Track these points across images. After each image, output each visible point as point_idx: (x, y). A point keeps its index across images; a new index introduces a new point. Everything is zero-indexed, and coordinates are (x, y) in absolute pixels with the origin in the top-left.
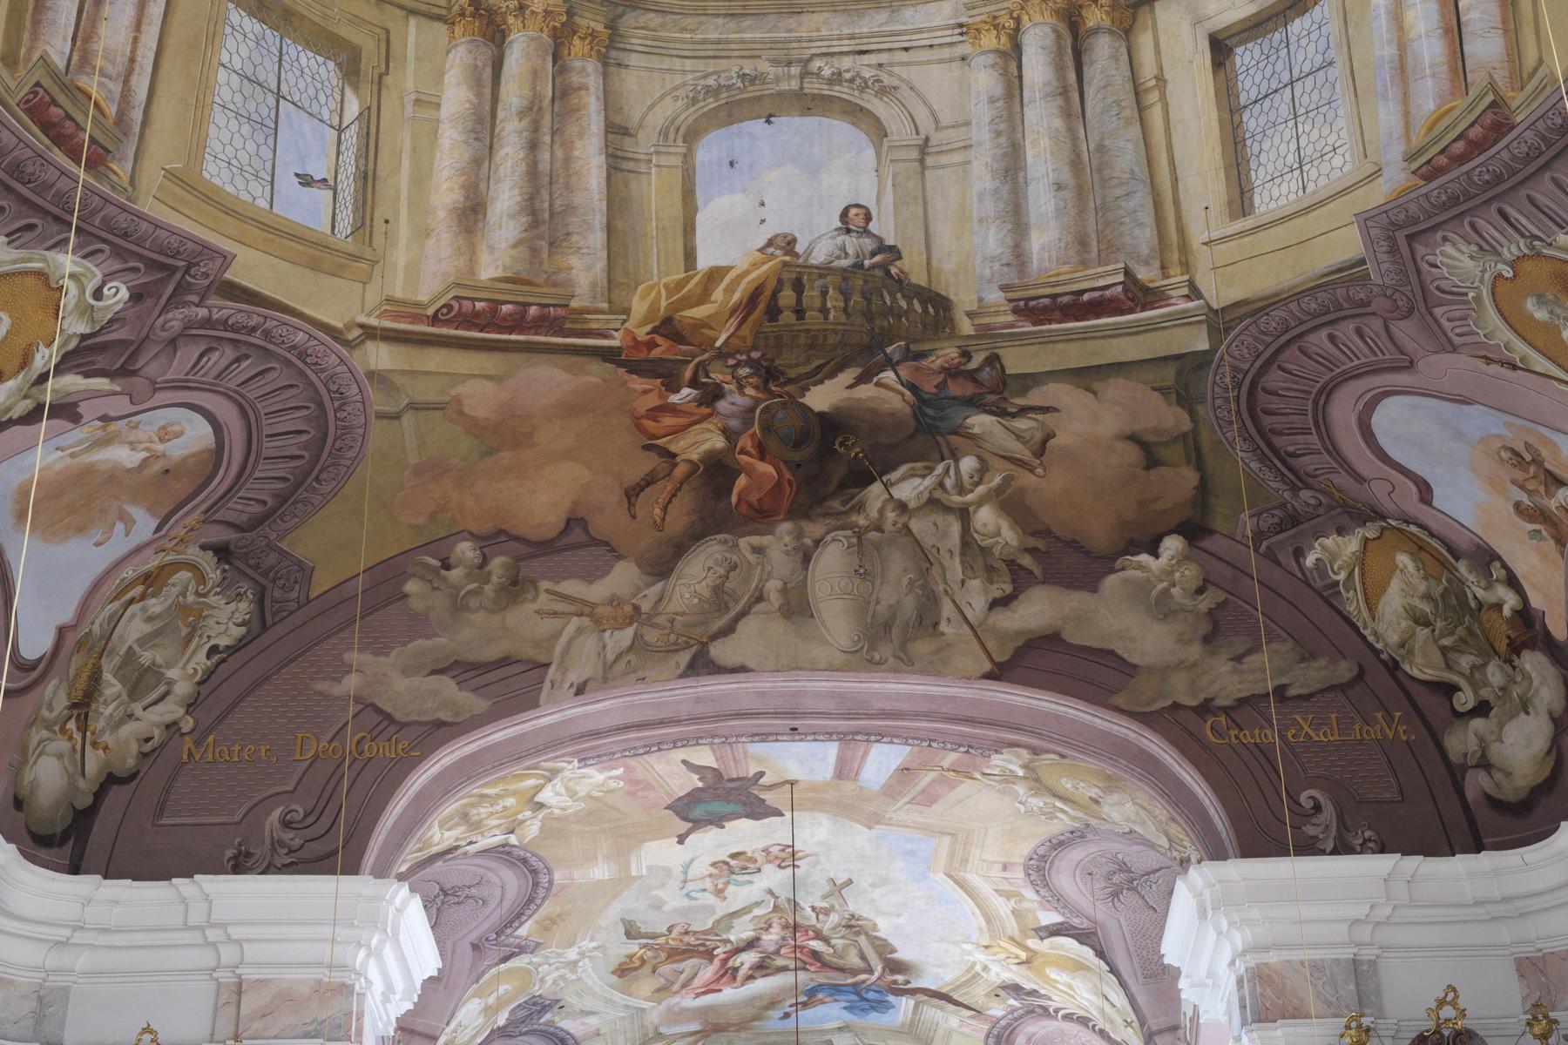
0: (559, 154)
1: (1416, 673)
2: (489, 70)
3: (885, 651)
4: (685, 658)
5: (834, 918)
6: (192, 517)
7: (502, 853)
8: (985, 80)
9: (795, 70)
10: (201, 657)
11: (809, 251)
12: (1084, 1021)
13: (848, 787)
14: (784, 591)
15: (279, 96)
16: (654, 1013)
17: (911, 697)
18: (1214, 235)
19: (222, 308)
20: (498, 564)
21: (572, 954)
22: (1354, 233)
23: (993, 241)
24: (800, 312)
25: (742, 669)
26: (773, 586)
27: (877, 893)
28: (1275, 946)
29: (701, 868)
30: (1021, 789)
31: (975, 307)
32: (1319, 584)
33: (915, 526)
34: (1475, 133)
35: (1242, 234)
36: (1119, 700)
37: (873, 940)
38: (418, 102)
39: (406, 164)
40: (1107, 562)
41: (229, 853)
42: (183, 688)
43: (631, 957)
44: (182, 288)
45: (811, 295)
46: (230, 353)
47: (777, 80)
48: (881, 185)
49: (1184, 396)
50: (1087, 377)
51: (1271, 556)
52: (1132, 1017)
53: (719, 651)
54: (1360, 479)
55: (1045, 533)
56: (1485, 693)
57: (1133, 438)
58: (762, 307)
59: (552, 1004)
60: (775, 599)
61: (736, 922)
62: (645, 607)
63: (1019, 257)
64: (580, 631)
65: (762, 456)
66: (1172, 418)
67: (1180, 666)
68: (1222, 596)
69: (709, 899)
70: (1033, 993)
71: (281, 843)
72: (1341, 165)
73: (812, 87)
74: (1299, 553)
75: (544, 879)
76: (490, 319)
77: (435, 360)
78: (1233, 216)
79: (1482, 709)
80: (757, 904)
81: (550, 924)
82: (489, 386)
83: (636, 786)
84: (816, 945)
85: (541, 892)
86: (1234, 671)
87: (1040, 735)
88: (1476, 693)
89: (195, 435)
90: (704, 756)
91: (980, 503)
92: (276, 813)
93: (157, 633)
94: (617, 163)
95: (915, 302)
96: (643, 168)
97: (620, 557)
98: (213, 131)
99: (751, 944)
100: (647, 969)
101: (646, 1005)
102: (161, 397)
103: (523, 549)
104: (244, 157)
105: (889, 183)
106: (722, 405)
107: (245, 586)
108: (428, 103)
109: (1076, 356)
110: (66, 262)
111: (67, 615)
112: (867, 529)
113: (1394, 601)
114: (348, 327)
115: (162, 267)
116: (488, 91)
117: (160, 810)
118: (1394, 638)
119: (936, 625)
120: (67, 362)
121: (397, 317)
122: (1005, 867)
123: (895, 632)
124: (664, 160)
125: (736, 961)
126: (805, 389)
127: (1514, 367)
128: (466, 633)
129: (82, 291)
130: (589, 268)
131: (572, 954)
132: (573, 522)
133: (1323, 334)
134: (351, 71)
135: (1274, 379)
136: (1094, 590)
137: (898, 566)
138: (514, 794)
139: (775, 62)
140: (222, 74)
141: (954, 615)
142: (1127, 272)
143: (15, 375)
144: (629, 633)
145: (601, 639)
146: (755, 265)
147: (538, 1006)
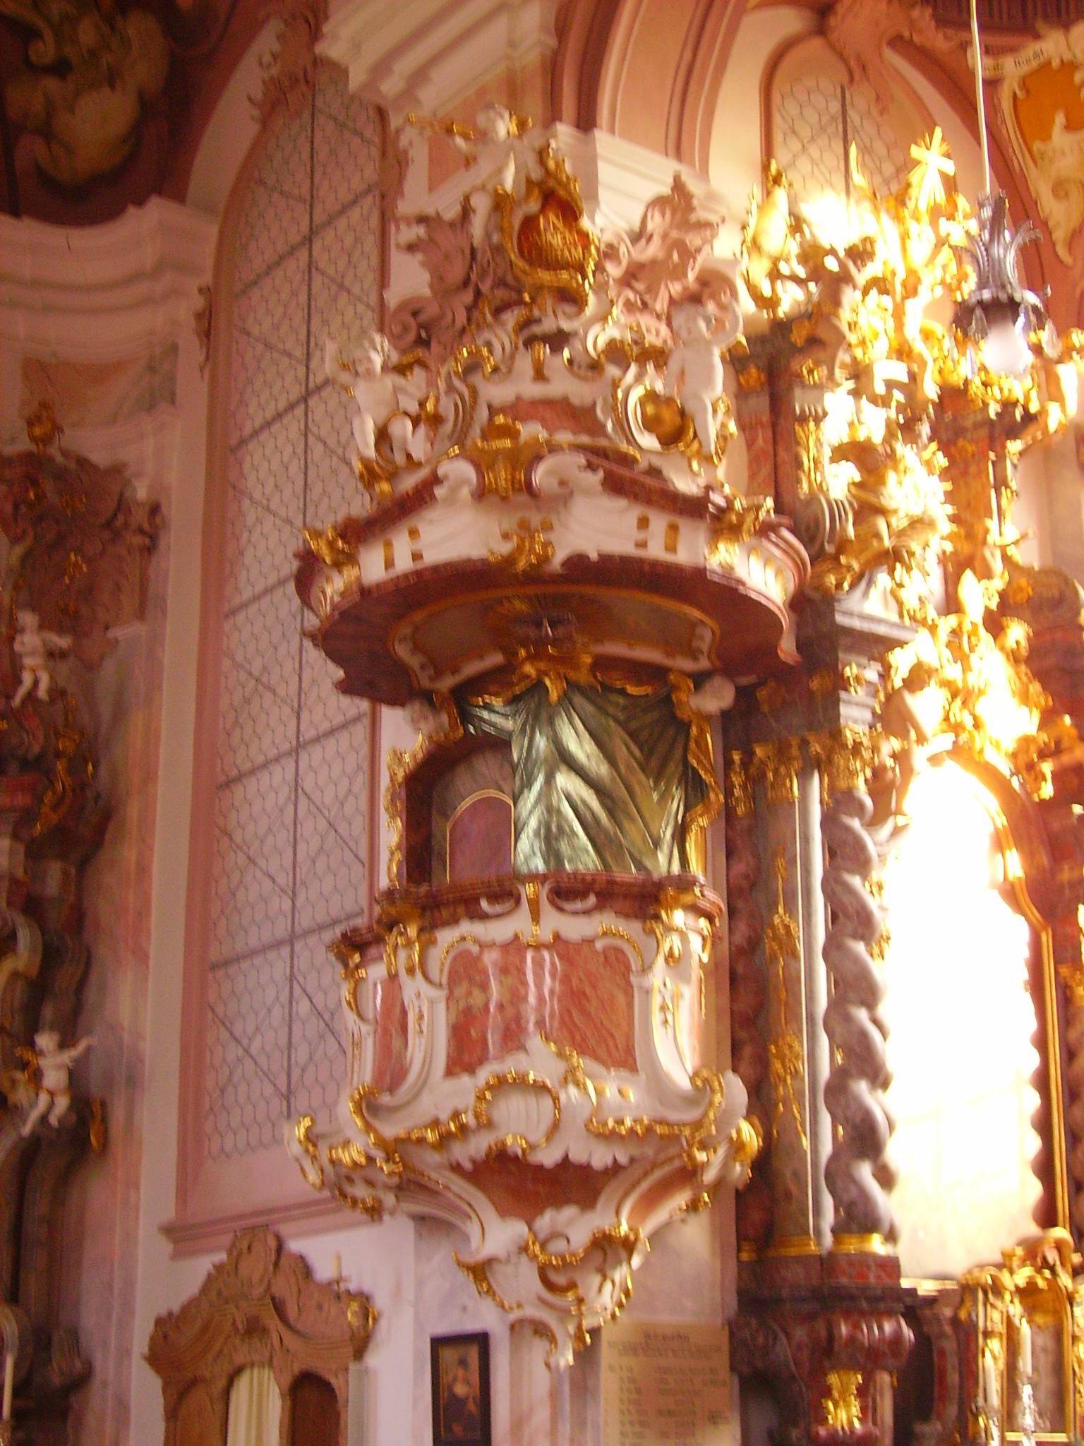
79: (61, 68)
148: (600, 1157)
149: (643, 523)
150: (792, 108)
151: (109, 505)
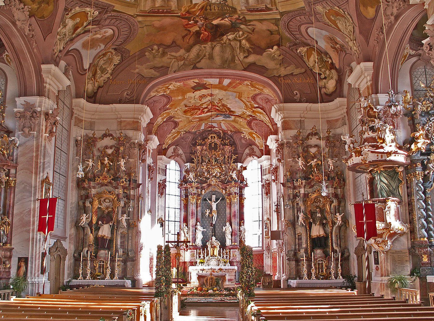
3: (226, 65)
4: (192, 66)
5: (220, 104)
7: (163, 95)
12: (262, 121)
13: (221, 85)
14: (209, 55)
19: (114, 14)
20: (161, 49)
21: (176, 110)
24: (211, 10)
26: (207, 54)
27: (227, 101)
31: (240, 10)
32: (300, 55)
33: (232, 43)
36: (265, 75)
37: (227, 108)
40: (264, 50)
42: (110, 71)
43: (186, 110)
44: (107, 11)
45: (212, 7)
46: (115, 20)
49: (277, 25)
50: (261, 21)
51: (292, 50)
53: (198, 65)
54: (306, 39)
55: (254, 45)
56: (326, 75)
57: (268, 30)
60: (207, 56)
64: (175, 61)
65: (205, 31)
67: (276, 69)
68: (283, 57)
69: (199, 101)
71: (127, 98)
74: (297, 50)
76: (158, 12)
77: (149, 19)
79: (325, 78)
80: (207, 102)
81: (172, 106)
82: (158, 22)
85: (170, 101)
86: (285, 70)
87: (252, 79)
88: (324, 75)
89: (110, 32)
90: (197, 81)
91: (243, 39)
97: (181, 48)
99: (206, 108)
101: (189, 117)
102: (104, 27)
103: (165, 47)
106: (198, 23)
107: (119, 54)
109: (258, 17)
110: (88, 9)
111: (91, 62)
112: (224, 44)
113: (312, 59)
114: (134, 15)
115: (103, 8)
117: (107, 93)
120: (89, 24)
123: (228, 62)
128: (156, 62)
129: (91, 13)
130: (174, 4)
131: (176, 110)
132: (174, 42)
133: (299, 17)
135: (291, 23)
136: (262, 55)
137: (228, 50)
138: (164, 87)
141: (238, 59)
143: (81, 27)
144: (183, 62)
145: (178, 63)
147: (171, 117)
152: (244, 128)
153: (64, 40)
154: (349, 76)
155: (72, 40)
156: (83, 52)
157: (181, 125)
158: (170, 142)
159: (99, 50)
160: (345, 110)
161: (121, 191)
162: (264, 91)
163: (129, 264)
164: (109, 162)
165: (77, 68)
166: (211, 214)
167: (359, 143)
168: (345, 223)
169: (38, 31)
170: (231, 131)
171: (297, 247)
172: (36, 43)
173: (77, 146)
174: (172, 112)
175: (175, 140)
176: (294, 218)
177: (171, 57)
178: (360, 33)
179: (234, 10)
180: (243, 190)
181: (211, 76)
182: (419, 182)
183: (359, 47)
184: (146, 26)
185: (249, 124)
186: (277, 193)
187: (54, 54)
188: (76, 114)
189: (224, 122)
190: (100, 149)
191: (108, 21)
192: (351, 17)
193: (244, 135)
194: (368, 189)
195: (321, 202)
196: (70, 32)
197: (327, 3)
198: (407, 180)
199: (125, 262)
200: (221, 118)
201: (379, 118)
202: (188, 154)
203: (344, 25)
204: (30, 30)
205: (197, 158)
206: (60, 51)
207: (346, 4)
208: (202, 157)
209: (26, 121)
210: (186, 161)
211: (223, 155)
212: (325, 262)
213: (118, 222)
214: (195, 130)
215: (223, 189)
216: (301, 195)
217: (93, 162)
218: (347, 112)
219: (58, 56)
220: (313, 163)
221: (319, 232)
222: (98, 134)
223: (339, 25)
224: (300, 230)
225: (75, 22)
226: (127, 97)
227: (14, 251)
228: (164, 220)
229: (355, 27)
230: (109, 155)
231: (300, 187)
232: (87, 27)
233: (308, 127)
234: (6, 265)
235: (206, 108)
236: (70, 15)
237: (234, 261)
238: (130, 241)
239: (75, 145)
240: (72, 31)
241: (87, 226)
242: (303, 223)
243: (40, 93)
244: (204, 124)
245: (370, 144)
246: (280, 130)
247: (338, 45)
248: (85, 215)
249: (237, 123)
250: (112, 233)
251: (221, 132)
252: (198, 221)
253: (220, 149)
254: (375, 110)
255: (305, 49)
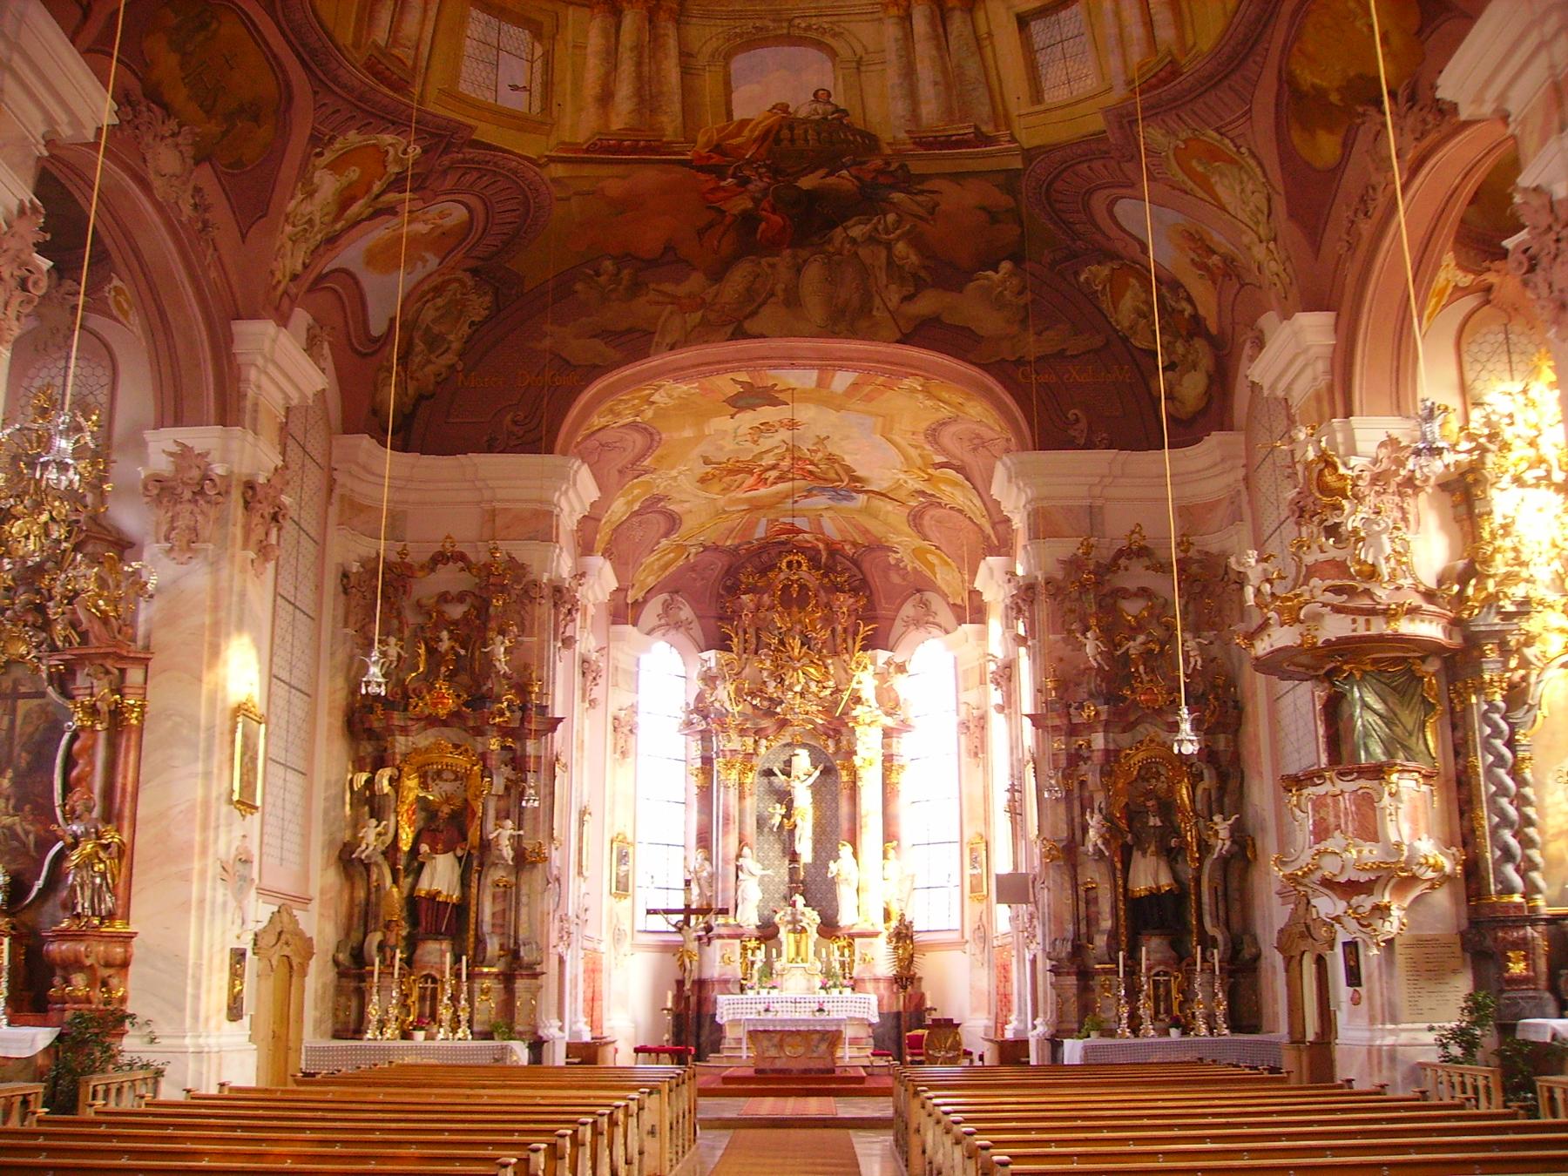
0: (654, 68)
1: (1138, 344)
2: (613, 30)
4: (730, 329)
5: (820, 455)
6: (458, 255)
7: (633, 426)
8: (892, 30)
9: (785, 24)
10: (466, 327)
11: (796, 112)
12: (960, 511)
13: (824, 392)
14: (785, 290)
15: (499, 49)
16: (722, 500)
17: (857, 351)
18: (1022, 112)
19: (471, 153)
20: (625, 273)
21: (674, 473)
22: (1100, 117)
23: (900, 107)
24: (792, 140)
25: (763, 336)
26: (780, 287)
27: (843, 443)
28: (1046, 498)
29: (744, 429)
30: (920, 396)
33: (862, 252)
34: (1162, 74)
35: (1038, 113)
38: (575, 47)
39: (569, 76)
40: (969, 275)
41: (485, 438)
42: (456, 345)
45: (799, 132)
46: (475, 175)
47: (775, 29)
48: (836, 78)
50: (956, 177)
52: (985, 513)
54: (1109, 238)
56: (1175, 358)
57: (983, 209)
58: (770, 139)
59: (666, 498)
60: (780, 293)
61: (765, 456)
62: (708, 299)
63: (915, 115)
64: (671, 313)
65: (774, 212)
66: (1005, 200)
69: (749, 445)
70: (933, 495)
72: (1090, 83)
73: (797, 32)
74: (1076, 274)
75: (657, 438)
76: (618, 149)
77: (587, 170)
78: (1033, 104)
83: (705, 391)
84: (810, 467)
85: (655, 444)
89: (458, 214)
90: (743, 377)
91: (898, 240)
92: (509, 417)
93: (442, 316)
94: (686, 71)
95: (858, 137)
96: (701, 72)
97: (694, 269)
98: (464, 69)
99: (774, 467)
100: (716, 480)
104: (480, 79)
105: (840, 80)
106: (751, 187)
108: (580, 47)
109: (948, 167)
110: (388, 138)
113: (1128, 303)
116: (613, 40)
118: (1126, 324)
119: (871, 311)
121: (566, 151)
122: (913, 434)
124: (713, 68)
125: (767, 475)
126: (797, 179)
127: (1186, 193)
132: (669, 248)
133: (1085, 165)
134: (537, 35)
139: (774, 21)
140: (468, 41)
142: (976, 127)
144: (700, 313)
146: (766, 118)
147: (658, 499)
148: (1363, 877)
149: (1354, 621)
150: (1475, 348)
151: (1222, 572)
152: (898, 533)
153: (307, 240)
154: (1252, 359)
155: (331, 241)
156: (370, 281)
157: (689, 523)
158: (651, 581)
159: (419, 273)
160: (1241, 473)
161: (494, 744)
162: (967, 409)
163: (520, 984)
164: (453, 648)
165: (348, 333)
166: (789, 819)
167: (1289, 582)
168: (1243, 848)
169: (221, 213)
170: (854, 544)
171: (1083, 929)
172: (216, 250)
173: (345, 591)
174: (660, 482)
175: (667, 573)
176: (1073, 830)
177: (661, 299)
178: (1292, 215)
179: (870, 142)
180: (895, 740)
181: (792, 361)
182: (1493, 707)
183: (1287, 264)
184: (575, 194)
185: (916, 519)
186: (1012, 749)
187: (275, 288)
188: (343, 486)
189: (830, 513)
190: (424, 601)
191: (449, 182)
192: (1261, 165)
193: (898, 556)
194: (1321, 731)
195: (1163, 778)
196: (327, 214)
197: (1180, 118)
198: (1451, 701)
199: (508, 979)
200: (821, 501)
201: (1355, 496)
202: (713, 621)
203: (1238, 189)
204: (195, 206)
205: (741, 633)
206: (295, 277)
207: (1241, 121)
208: (758, 629)
209: (179, 507)
210: (702, 644)
211: (828, 621)
212: (1176, 978)
213: (486, 846)
214: (737, 542)
215: (829, 737)
216: (1096, 753)
217: (402, 647)
218: (1246, 479)
219: (285, 293)
220: (1134, 646)
221: (1156, 879)
222: (419, 554)
223: (1220, 190)
224: (1094, 875)
225: (344, 181)
226: (515, 429)
227: (136, 944)
228: (630, 839)
229: (1275, 197)
230: (456, 623)
231: (1090, 727)
232: (382, 199)
233: (1117, 530)
234: (109, 991)
235: (774, 467)
236: (329, 157)
237: (866, 975)
238: (524, 911)
239: (340, 589)
240: (333, 208)
241: (380, 859)
242: (1103, 847)
243: (229, 410)
244: (764, 521)
245: (1329, 582)
246: (1021, 539)
247: (1215, 258)
248: (373, 822)
249: (876, 517)
250: (465, 882)
251: (821, 546)
252: (746, 844)
253: (817, 605)
254: (1342, 470)
255: (1105, 271)
